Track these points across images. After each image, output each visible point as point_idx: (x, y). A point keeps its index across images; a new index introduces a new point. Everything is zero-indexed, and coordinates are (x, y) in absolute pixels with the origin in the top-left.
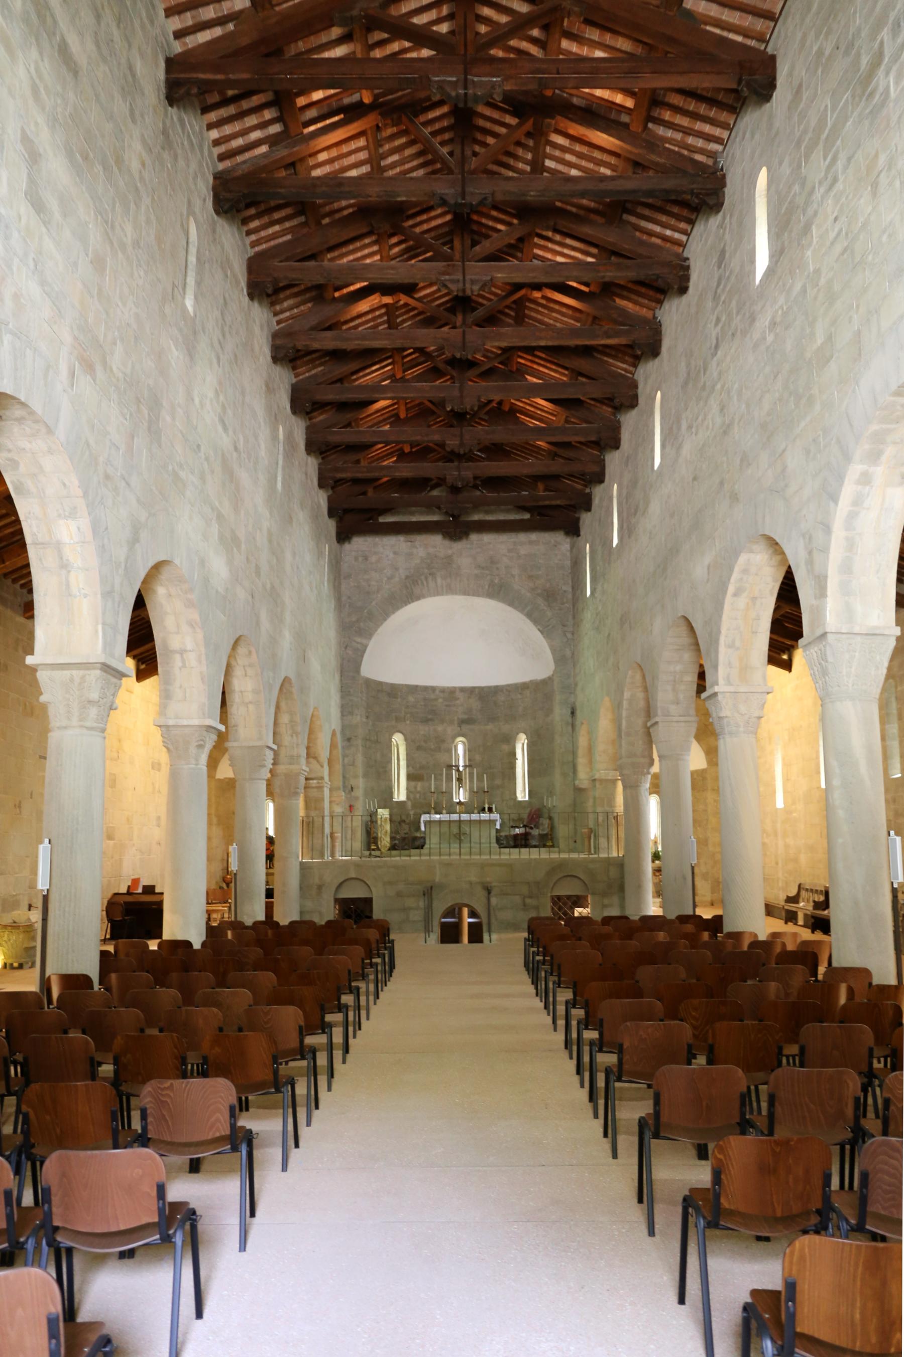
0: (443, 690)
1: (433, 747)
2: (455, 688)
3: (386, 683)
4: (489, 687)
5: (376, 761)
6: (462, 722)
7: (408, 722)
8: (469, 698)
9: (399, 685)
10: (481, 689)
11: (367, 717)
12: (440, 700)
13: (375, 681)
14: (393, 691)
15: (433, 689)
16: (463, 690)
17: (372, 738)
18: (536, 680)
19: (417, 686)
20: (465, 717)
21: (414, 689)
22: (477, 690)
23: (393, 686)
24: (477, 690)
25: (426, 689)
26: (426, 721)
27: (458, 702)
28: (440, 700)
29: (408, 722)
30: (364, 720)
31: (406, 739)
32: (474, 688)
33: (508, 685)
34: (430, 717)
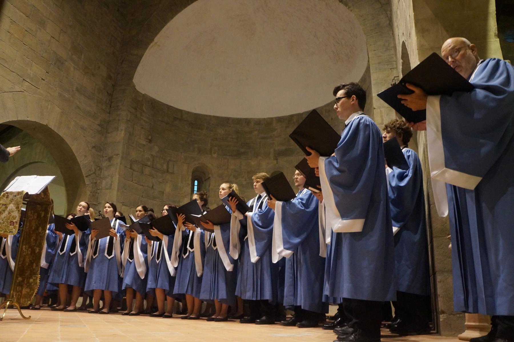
0: (259, 122)
1: (244, 183)
2: (272, 118)
3: (188, 113)
5: (162, 193)
7: (215, 155)
8: (287, 127)
11: (150, 141)
12: (256, 133)
13: (169, 107)
15: (247, 121)
17: (159, 166)
19: (228, 119)
20: (283, 148)
22: (295, 119)
24: (295, 119)
25: (239, 121)
26: (238, 155)
27: (275, 133)
28: (256, 133)
29: (215, 155)
30: (144, 143)
32: (292, 116)
34: (242, 150)
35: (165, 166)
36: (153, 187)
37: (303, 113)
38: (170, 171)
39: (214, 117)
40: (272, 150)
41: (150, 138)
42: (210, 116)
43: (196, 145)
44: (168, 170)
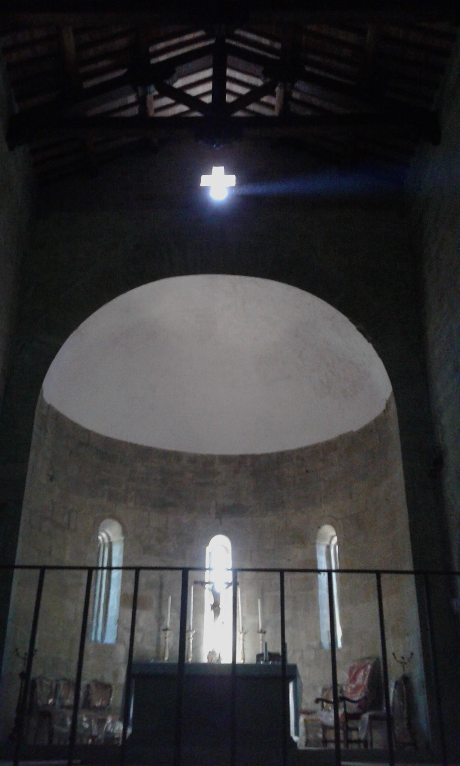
0: (194, 459)
3: (97, 435)
4: (268, 456)
6: (223, 512)
7: (131, 504)
8: (236, 472)
9: (120, 443)
10: (255, 458)
11: (52, 478)
13: (74, 425)
14: (109, 451)
15: (177, 456)
16: (226, 460)
18: (351, 432)
21: (145, 453)
23: (108, 442)
25: (166, 455)
26: (162, 506)
29: (131, 504)
31: (124, 532)
32: (243, 458)
33: (301, 450)
35: (66, 519)
36: (50, 553)
37: (261, 455)
38: (72, 526)
39: (131, 444)
40: (213, 503)
41: (51, 473)
42: (126, 443)
43: (106, 487)
44: (69, 525)
